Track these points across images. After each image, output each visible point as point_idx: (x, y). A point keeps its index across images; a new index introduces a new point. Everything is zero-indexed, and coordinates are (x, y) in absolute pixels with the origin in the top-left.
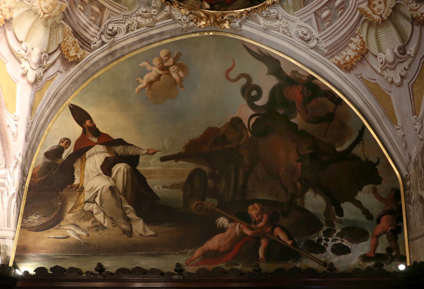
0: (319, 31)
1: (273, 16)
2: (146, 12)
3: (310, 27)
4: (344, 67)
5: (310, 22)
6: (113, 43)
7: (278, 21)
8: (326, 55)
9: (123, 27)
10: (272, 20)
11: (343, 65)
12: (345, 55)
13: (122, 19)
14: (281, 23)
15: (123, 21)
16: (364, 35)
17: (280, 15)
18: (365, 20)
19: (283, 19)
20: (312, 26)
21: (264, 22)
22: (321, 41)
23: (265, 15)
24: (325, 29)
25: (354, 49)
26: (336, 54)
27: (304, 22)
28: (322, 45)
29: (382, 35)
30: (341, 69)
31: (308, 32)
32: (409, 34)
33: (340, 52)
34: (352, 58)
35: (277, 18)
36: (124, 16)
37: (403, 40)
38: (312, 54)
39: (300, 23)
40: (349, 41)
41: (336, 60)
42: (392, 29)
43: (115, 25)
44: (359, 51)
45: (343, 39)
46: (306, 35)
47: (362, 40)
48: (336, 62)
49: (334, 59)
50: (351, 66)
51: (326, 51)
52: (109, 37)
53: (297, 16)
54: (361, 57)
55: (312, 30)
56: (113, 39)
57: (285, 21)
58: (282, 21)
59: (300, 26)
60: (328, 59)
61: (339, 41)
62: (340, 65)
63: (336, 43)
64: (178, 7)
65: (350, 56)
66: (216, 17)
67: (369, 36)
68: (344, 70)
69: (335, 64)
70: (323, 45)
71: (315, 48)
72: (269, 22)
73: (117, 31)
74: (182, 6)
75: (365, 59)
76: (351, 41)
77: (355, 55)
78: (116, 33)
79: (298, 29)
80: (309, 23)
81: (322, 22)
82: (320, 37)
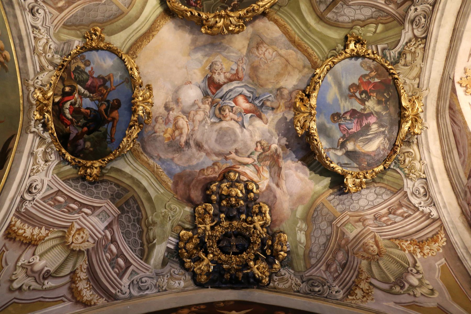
0: (43, 199)
1: (48, 157)
2: (50, 48)
3: (44, 190)
4: (10, 232)
5: (50, 189)
6: (22, 8)
7: (44, 162)
8: (18, 211)
9: (39, 24)
10: (43, 158)
11: (12, 230)
12: (25, 228)
13: (47, 24)
14: (42, 165)
15: (44, 25)
16: (51, 236)
17: (50, 163)
18: (65, 232)
19: (47, 167)
20: (46, 191)
21: (40, 151)
22: (33, 203)
23: (47, 151)
24: (45, 203)
25: (33, 234)
26: (22, 220)
27: (48, 185)
28: (28, 206)
29: (56, 251)
30: (6, 229)
31: (39, 189)
32: (62, 274)
33: (26, 222)
34: (23, 235)
35: (46, 161)
36: (50, 27)
37: (57, 271)
38: (15, 199)
39: (46, 181)
40: (40, 226)
41: (16, 222)
42: (63, 256)
43: (42, 17)
44: (33, 238)
45: (41, 220)
46: (35, 188)
47: (45, 237)
48: (13, 223)
49: (16, 219)
50: (13, 237)
51: (23, 210)
52: (30, 6)
53: (52, 177)
54: (28, 242)
55: (41, 193)
56: (28, 10)
57: (45, 169)
58: (45, 166)
59: (42, 182)
60: (14, 215)
61: (37, 218)
62: (11, 228)
63: (35, 216)
64: (56, 75)
65: (25, 232)
66: (46, 105)
67: (52, 240)
68: (7, 232)
69: (10, 222)
70: (28, 206)
71: (23, 200)
72: (41, 155)
73: (35, 16)
74: (57, 78)
75: (26, 246)
76: (41, 228)
77: (27, 237)
78: (33, 15)
79: (39, 181)
80: (48, 189)
81: (52, 198)
82: (36, 201)
